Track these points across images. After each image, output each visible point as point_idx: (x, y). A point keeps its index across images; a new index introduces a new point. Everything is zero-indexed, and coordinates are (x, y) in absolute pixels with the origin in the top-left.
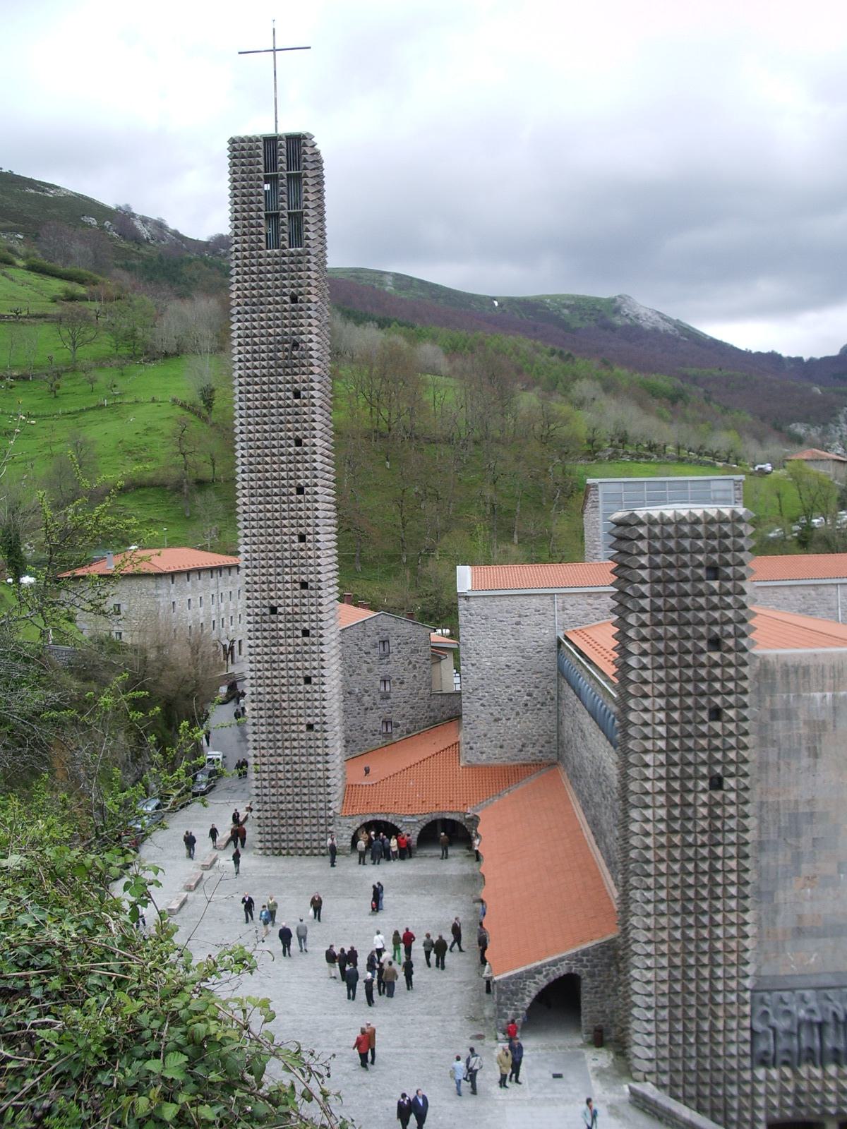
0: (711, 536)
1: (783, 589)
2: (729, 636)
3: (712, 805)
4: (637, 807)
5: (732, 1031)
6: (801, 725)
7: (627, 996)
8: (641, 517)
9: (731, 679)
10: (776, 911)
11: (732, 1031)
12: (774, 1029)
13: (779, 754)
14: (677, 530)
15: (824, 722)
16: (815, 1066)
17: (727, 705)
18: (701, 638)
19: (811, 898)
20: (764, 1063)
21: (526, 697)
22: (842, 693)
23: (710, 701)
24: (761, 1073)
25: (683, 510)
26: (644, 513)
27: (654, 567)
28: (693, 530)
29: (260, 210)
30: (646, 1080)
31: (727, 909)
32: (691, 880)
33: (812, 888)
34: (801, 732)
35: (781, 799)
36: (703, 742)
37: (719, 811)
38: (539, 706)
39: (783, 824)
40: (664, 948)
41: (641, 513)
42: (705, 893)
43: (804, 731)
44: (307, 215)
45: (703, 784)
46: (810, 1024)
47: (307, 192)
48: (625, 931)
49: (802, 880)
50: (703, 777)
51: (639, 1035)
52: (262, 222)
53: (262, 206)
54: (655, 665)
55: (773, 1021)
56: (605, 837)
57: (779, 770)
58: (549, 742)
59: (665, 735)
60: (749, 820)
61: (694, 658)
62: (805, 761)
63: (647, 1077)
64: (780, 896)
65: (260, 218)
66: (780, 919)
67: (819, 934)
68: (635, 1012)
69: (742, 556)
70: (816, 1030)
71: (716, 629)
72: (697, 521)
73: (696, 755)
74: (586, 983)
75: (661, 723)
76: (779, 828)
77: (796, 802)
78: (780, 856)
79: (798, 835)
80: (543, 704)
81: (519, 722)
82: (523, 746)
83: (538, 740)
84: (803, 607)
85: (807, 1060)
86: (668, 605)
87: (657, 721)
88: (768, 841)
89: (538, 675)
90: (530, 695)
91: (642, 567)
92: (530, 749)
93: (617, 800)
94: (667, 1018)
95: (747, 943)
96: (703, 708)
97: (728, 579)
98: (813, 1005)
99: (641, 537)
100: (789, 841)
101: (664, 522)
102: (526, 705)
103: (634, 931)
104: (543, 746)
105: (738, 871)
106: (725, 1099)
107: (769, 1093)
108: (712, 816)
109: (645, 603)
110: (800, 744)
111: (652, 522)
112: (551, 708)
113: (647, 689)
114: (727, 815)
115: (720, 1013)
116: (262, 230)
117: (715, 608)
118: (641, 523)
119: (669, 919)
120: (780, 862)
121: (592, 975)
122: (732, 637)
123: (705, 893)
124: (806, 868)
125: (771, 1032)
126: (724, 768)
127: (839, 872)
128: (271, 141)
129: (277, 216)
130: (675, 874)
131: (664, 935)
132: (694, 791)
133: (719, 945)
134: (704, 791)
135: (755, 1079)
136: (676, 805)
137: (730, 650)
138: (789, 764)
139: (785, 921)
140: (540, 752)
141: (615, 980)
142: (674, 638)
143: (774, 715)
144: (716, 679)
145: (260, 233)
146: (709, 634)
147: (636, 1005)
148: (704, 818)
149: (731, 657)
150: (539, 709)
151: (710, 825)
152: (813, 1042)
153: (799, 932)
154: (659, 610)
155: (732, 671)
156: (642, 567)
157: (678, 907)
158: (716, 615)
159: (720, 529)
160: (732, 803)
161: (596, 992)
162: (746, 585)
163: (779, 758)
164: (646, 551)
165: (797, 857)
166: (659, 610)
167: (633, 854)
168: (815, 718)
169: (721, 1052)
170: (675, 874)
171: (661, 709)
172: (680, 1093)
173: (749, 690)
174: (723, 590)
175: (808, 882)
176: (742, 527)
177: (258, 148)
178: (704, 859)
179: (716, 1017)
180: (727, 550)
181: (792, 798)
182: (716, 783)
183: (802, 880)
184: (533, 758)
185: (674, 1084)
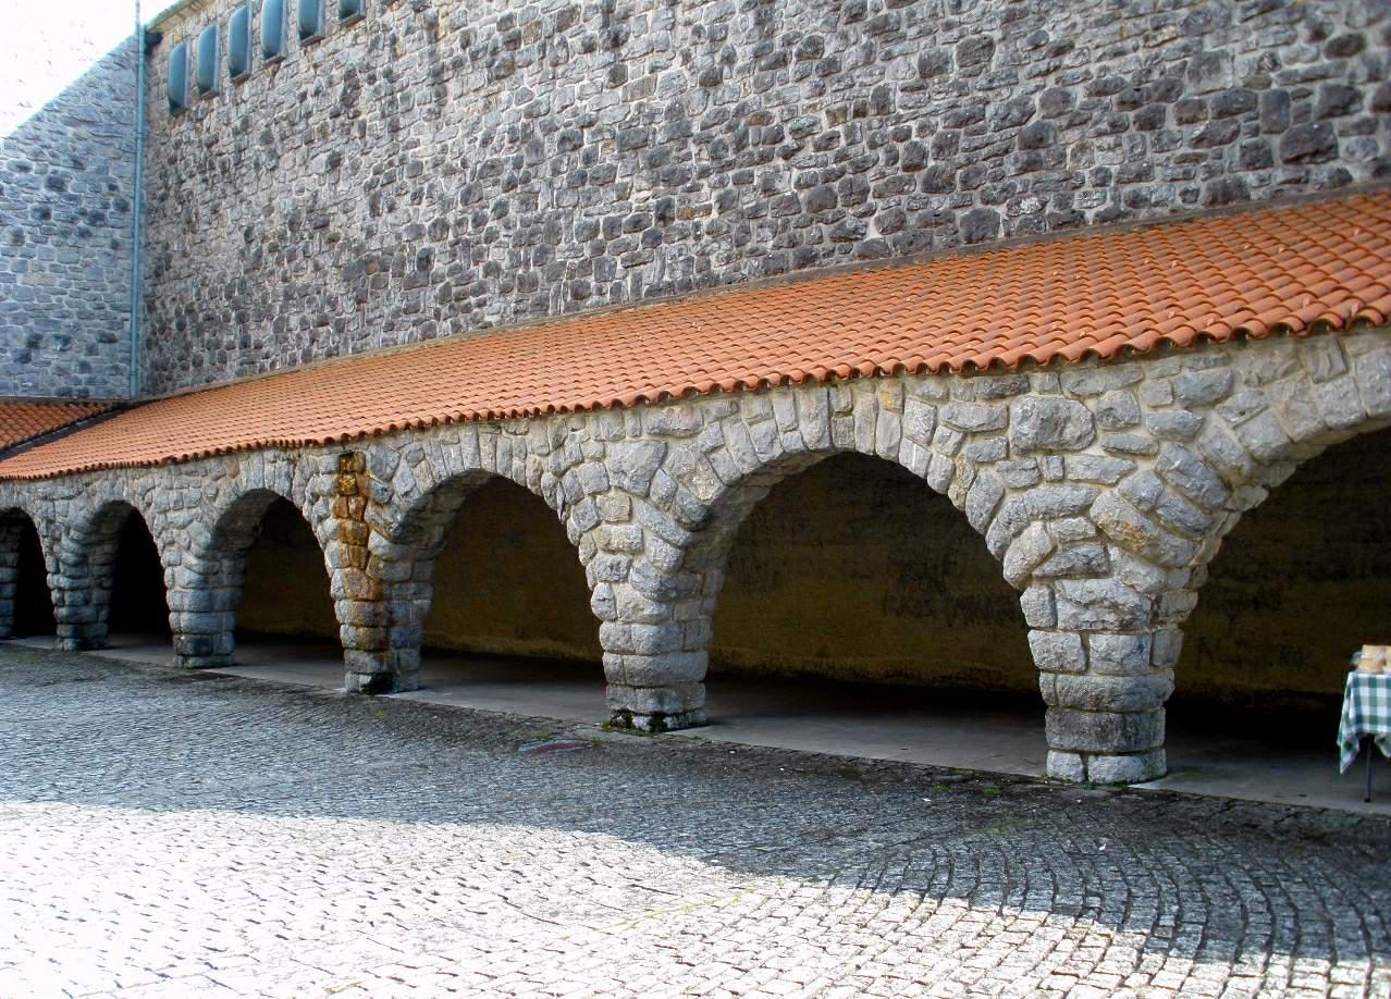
21: (44, 192)
38: (81, 224)
58: (111, 340)
80: (96, 219)
81: (22, 268)
82: (34, 343)
83: (77, 327)
89: (84, 130)
90: (56, 184)
92: (50, 354)
102: (46, 215)
104: (91, 350)
112: (117, 235)
140: (84, 367)
150: (84, 234)
184: (62, 383)
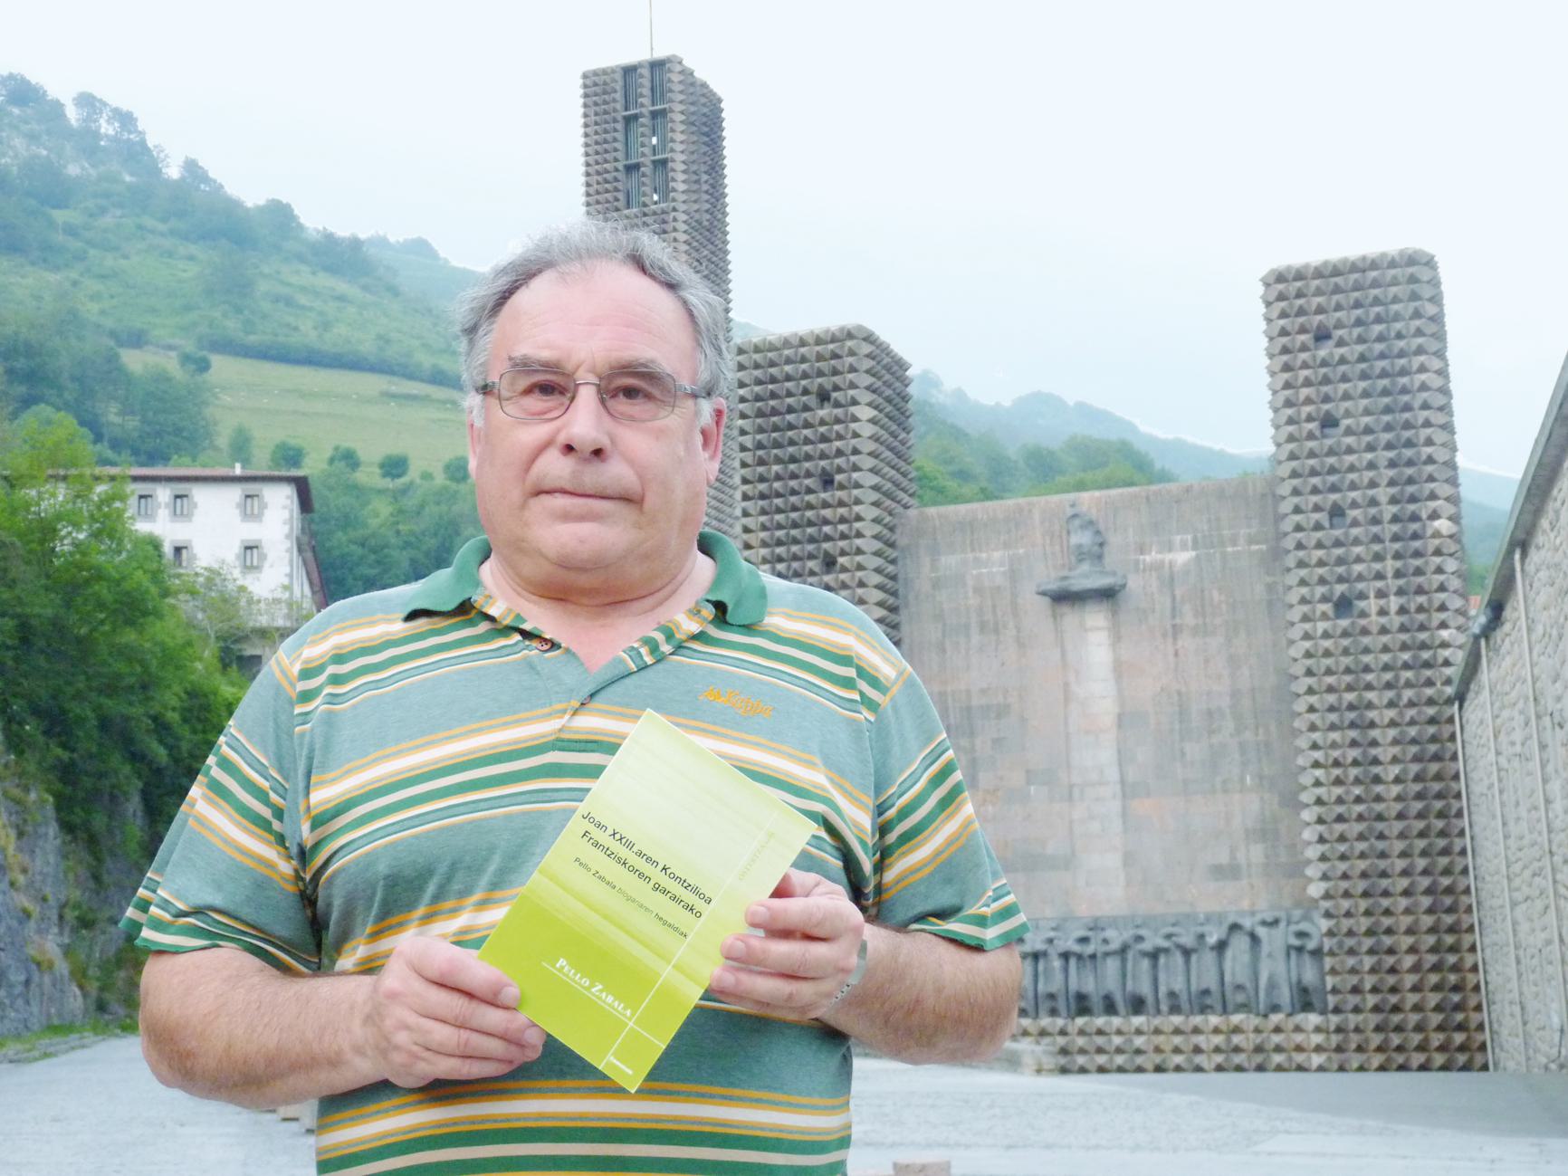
15: (999, 588)
22: (1021, 551)
29: (616, 160)
34: (971, 602)
35: (949, 689)
43: (973, 601)
44: (673, 161)
47: (673, 130)
52: (620, 176)
53: (620, 155)
57: (944, 651)
62: (976, 638)
65: (617, 170)
77: (968, 692)
79: (972, 734)
116: (620, 186)
127: (1029, 783)
128: (629, 71)
129: (637, 167)
143: (936, 584)
145: (616, 190)
163: (944, 636)
177: (614, 81)
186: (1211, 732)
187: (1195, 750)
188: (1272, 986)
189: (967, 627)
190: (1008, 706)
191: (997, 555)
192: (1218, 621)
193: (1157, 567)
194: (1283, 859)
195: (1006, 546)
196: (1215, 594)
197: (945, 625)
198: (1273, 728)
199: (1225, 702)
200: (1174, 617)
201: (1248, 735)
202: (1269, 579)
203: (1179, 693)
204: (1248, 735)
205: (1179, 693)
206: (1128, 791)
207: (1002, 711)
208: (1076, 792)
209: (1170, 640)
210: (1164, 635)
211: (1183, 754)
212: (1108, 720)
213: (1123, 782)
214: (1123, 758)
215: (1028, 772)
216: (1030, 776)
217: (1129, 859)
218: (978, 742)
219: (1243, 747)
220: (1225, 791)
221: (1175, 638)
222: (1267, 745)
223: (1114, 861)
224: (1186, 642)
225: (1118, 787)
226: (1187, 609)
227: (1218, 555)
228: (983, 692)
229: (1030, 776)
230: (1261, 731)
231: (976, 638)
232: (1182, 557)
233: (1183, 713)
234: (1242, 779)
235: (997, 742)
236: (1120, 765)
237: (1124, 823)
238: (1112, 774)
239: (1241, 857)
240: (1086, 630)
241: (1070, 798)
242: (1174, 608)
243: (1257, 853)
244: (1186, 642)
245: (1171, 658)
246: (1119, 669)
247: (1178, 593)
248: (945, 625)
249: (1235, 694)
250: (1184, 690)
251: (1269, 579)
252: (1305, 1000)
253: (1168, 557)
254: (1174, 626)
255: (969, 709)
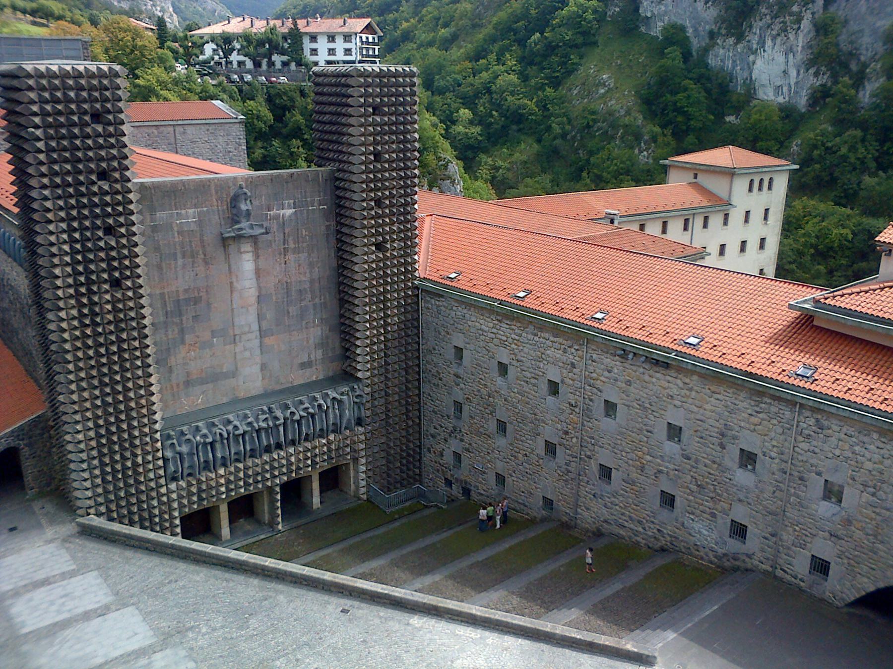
0: (92, 88)
1: (144, 128)
2: (115, 169)
3: (114, 302)
4: (51, 310)
5: (149, 462)
6: (176, 235)
7: (63, 453)
8: (28, 69)
9: (119, 204)
10: (170, 370)
11: (149, 462)
12: (180, 454)
13: (161, 258)
14: (63, 83)
16: (211, 471)
17: (118, 224)
18: (91, 172)
19: (195, 358)
20: (174, 479)
23: (104, 222)
24: (173, 486)
25: (68, 66)
26: (31, 66)
27: (44, 114)
28: (77, 83)
30: (88, 514)
31: (136, 376)
32: (104, 360)
33: (194, 351)
34: (177, 240)
35: (166, 291)
36: (102, 255)
37: (120, 306)
39: (169, 309)
40: (89, 414)
41: (29, 67)
42: (117, 368)
45: (106, 287)
46: (205, 444)
48: (54, 405)
49: (187, 346)
50: (105, 281)
51: (77, 482)
54: (55, 196)
55: (178, 448)
56: (17, 334)
59: (69, 251)
60: (145, 309)
61: (87, 188)
63: (89, 511)
64: (172, 361)
66: (174, 375)
67: (203, 381)
68: (72, 466)
69: (121, 104)
70: (209, 448)
71: (104, 165)
72: (80, 75)
73: (96, 264)
74: (25, 452)
75: (65, 242)
76: (167, 313)
77: (177, 291)
78: (170, 332)
79: (180, 315)
84: (149, 142)
85: (204, 469)
86: (61, 146)
87: (61, 241)
88: (159, 323)
91: (35, 114)
93: (31, 306)
94: (98, 465)
95: (154, 399)
96: (99, 228)
97: (109, 123)
98: (205, 431)
99: (30, 88)
100: (175, 320)
101: (51, 75)
103: (63, 406)
105: (141, 348)
106: (150, 511)
107: (180, 497)
108: (115, 310)
109: (40, 145)
110: (176, 249)
111: (41, 75)
113: (50, 216)
114: (127, 307)
115: (139, 452)
117: (101, 147)
118: (29, 76)
119: (90, 392)
120: (170, 337)
121: (28, 445)
122: (117, 170)
123: (117, 368)
124: (189, 338)
125: (178, 456)
126: (121, 273)
130: (91, 358)
131: (88, 405)
132: (100, 292)
133: (133, 404)
134: (107, 292)
135: (169, 491)
136: (85, 305)
137: (116, 181)
138: (170, 264)
139: (178, 376)
141: (48, 444)
142: (68, 173)
144: (107, 204)
146: (98, 169)
147: (71, 461)
148: (109, 312)
149: (118, 186)
151: (114, 317)
152: (208, 456)
153: (188, 383)
154: (54, 150)
155: (120, 197)
156: (35, 114)
157: (96, 382)
158: (103, 153)
159: (100, 82)
160: (130, 299)
161: (34, 457)
162: (125, 128)
164: (37, 100)
165: (182, 331)
166: (54, 150)
167: (53, 347)
168: (186, 229)
169: (142, 479)
170: (91, 358)
171: (64, 231)
172: (115, 515)
173: (135, 211)
174: (107, 133)
175: (192, 348)
176: (118, 81)
178: (113, 343)
179: (136, 456)
180: (107, 100)
181: (174, 289)
182: (116, 284)
183: (187, 346)
185: (109, 511)
186: (301, 300)
187: (293, 310)
188: (349, 420)
189: (175, 254)
190: (201, 297)
191: (191, 211)
192: (305, 245)
193: (277, 217)
194: (330, 355)
195: (196, 206)
196: (304, 231)
197: (161, 254)
198: (327, 296)
199: (307, 286)
200: (284, 245)
201: (317, 300)
202: (328, 223)
203: (287, 283)
204: (317, 300)
205: (287, 283)
206: (263, 333)
207: (196, 301)
208: (237, 338)
209: (283, 256)
210: (280, 254)
211: (288, 313)
212: (253, 300)
213: (260, 330)
214: (260, 317)
215: (212, 331)
216: (214, 334)
217: (263, 367)
218: (184, 318)
219: (315, 305)
220: (307, 328)
221: (285, 255)
222: (325, 303)
223: (256, 369)
224: (291, 257)
225: (258, 333)
226: (290, 240)
227: (305, 211)
228: (186, 291)
229: (214, 334)
230: (322, 298)
231: (180, 262)
232: (289, 212)
233: (288, 293)
234: (314, 321)
235: (196, 318)
236: (259, 322)
237: (261, 350)
238: (255, 327)
239: (313, 357)
240: (241, 253)
241: (235, 342)
242: (284, 240)
243: (320, 353)
244: (291, 257)
245: (283, 265)
246: (258, 272)
247: (286, 231)
248: (161, 254)
249: (312, 281)
250: (289, 281)
251: (328, 223)
252: (359, 422)
253: (282, 212)
254: (284, 248)
255: (178, 301)
